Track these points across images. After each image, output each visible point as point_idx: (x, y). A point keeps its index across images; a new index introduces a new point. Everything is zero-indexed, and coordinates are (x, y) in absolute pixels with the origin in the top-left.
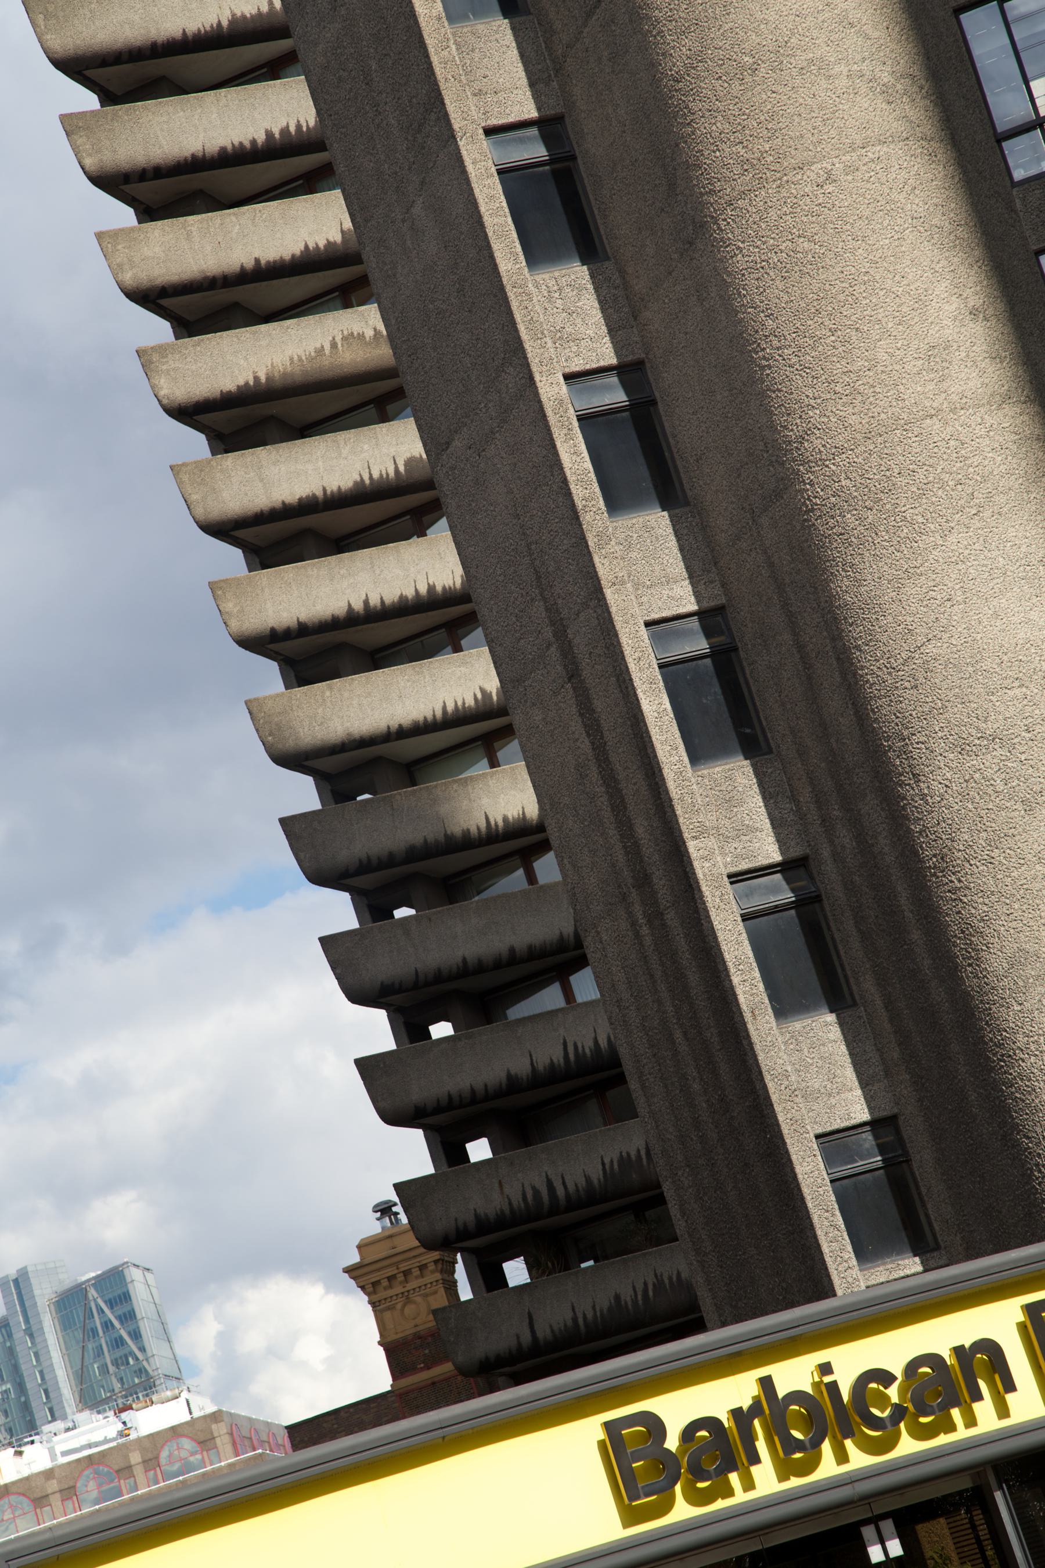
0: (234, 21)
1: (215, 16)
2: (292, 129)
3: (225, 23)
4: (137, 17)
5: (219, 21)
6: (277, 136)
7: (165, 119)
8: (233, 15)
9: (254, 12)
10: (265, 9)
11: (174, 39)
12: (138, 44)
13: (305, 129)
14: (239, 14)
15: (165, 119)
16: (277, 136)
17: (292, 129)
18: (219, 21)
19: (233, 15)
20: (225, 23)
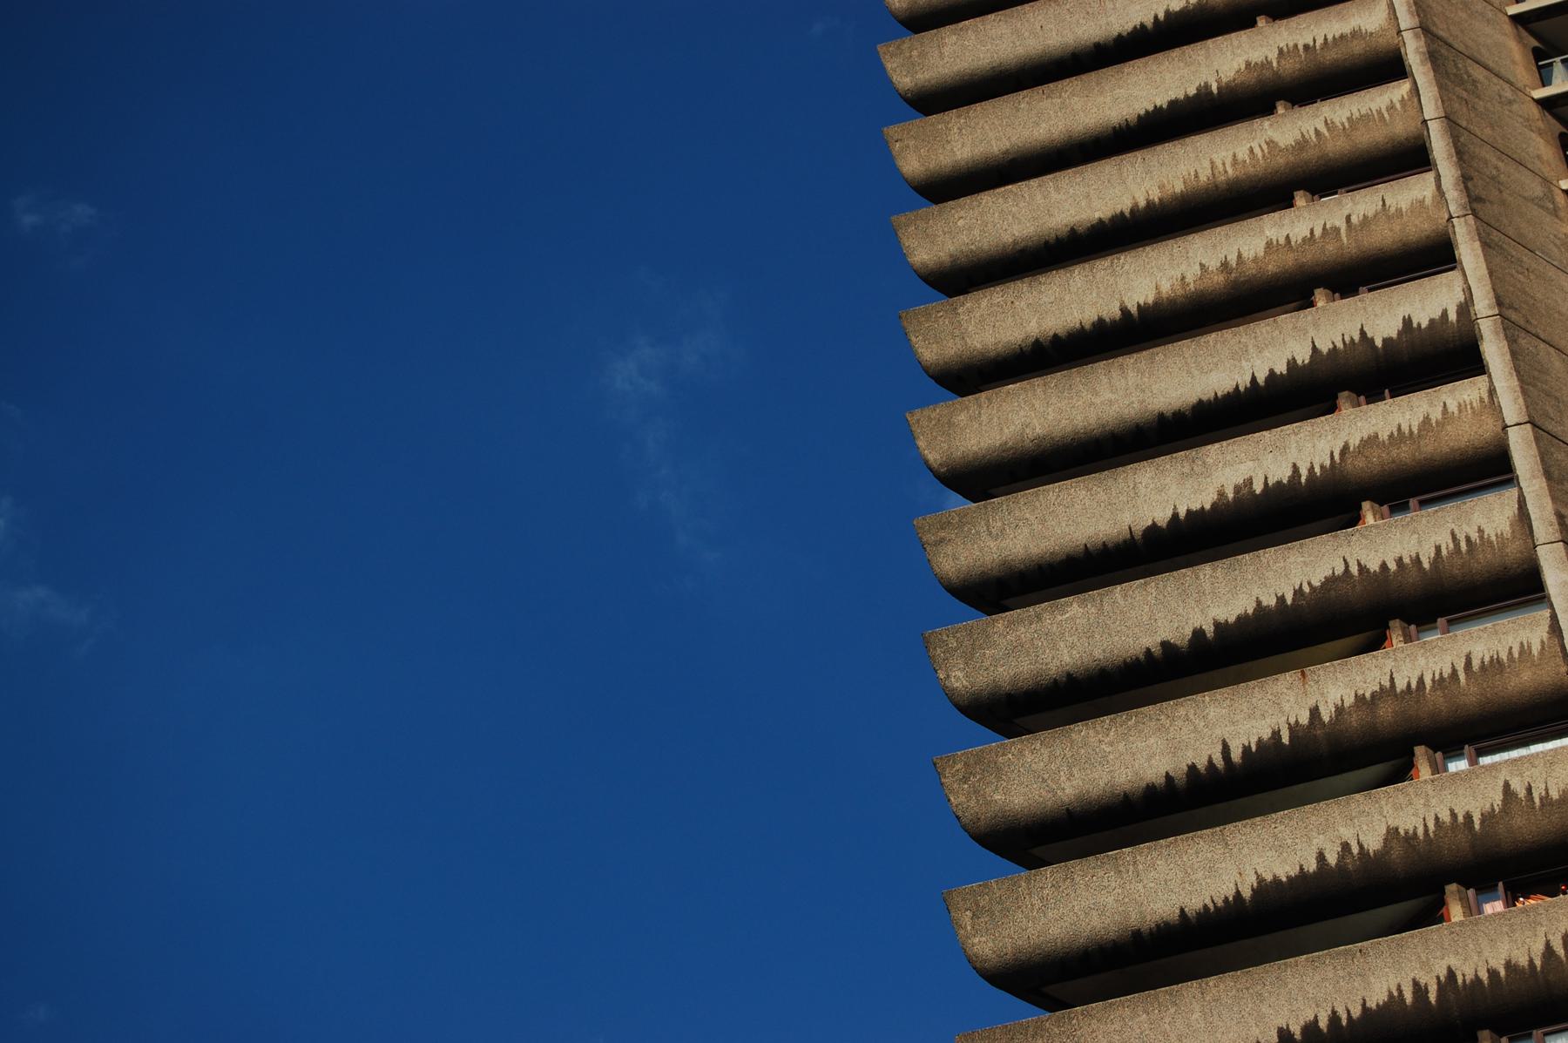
0: (1266, 890)
1: (1232, 886)
2: (1323, 1024)
3: (1247, 893)
4: (1110, 899)
5: (1238, 892)
6: (1298, 1036)
7: (1117, 1026)
8: (1260, 880)
9: (1294, 872)
10: (1312, 866)
11: (1166, 924)
12: (1112, 936)
13: (1344, 1022)
14: (1269, 878)
15: (1117, 1026)
16: (1298, 1036)
17: (1323, 1024)
18: (1238, 892)
19: (1260, 880)
20: (1247, 893)
